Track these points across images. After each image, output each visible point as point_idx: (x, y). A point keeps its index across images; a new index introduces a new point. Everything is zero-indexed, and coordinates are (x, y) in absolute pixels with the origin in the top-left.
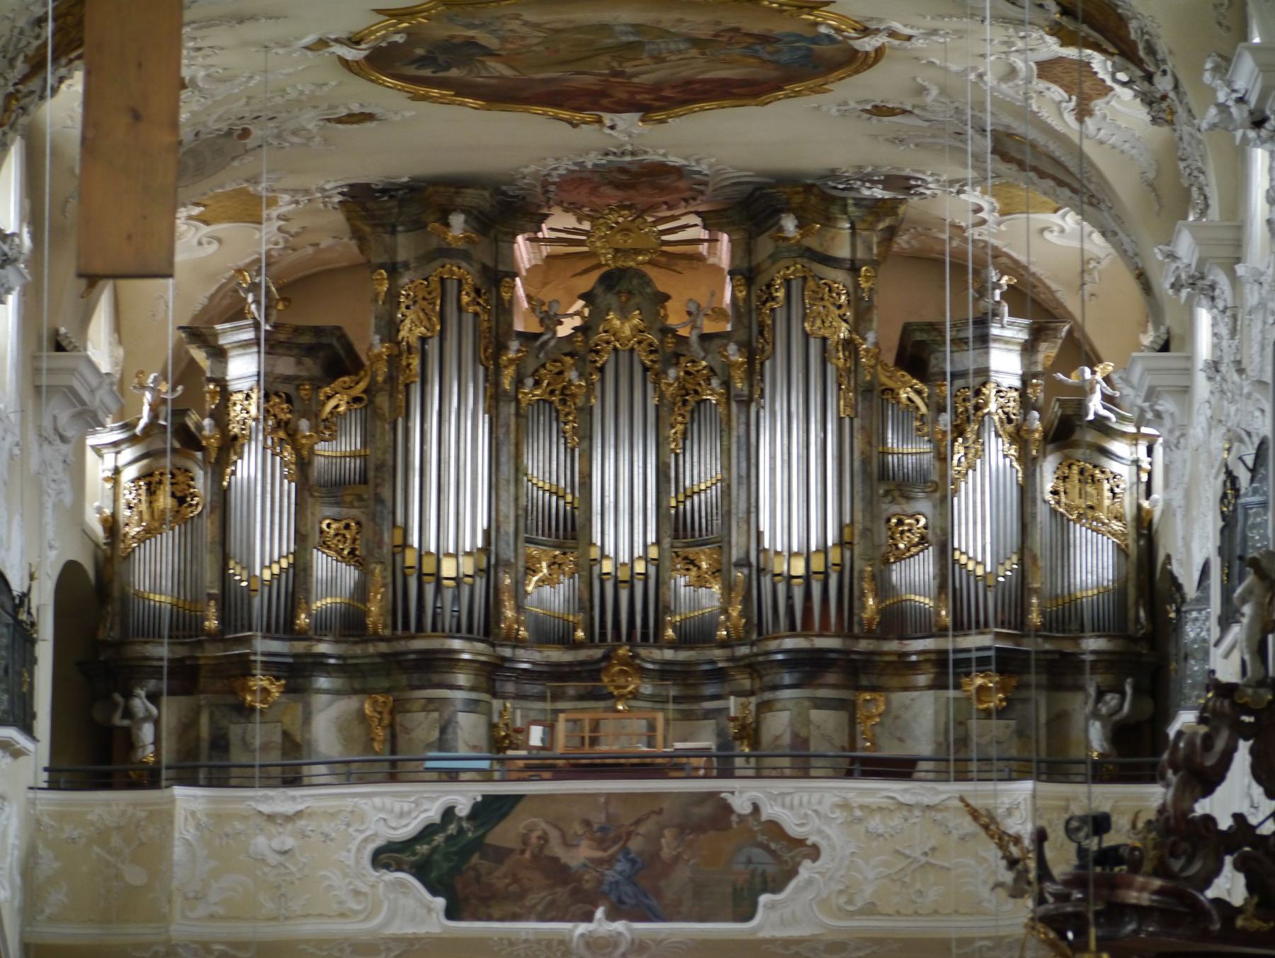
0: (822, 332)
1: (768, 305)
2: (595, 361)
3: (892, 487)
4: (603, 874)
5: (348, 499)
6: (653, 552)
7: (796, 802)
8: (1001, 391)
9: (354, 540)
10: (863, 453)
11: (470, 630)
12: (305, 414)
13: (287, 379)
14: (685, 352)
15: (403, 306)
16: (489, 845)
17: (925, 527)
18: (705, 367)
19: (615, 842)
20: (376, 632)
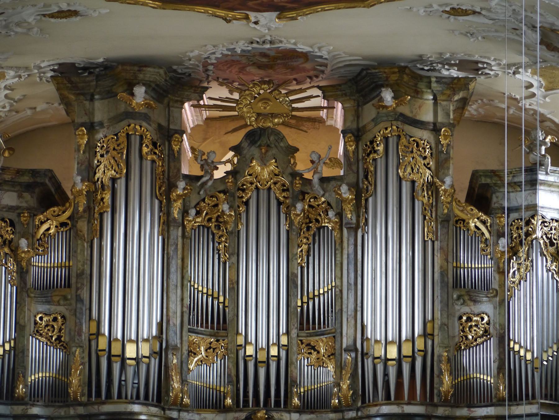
1: (371, 156)
2: (242, 197)
3: (463, 293)
5: (56, 299)
6: (284, 340)
8: (546, 222)
9: (60, 330)
10: (441, 267)
11: (146, 397)
12: (24, 235)
13: (11, 209)
14: (309, 191)
15: (99, 154)
17: (488, 323)
18: (324, 202)
20: (75, 399)
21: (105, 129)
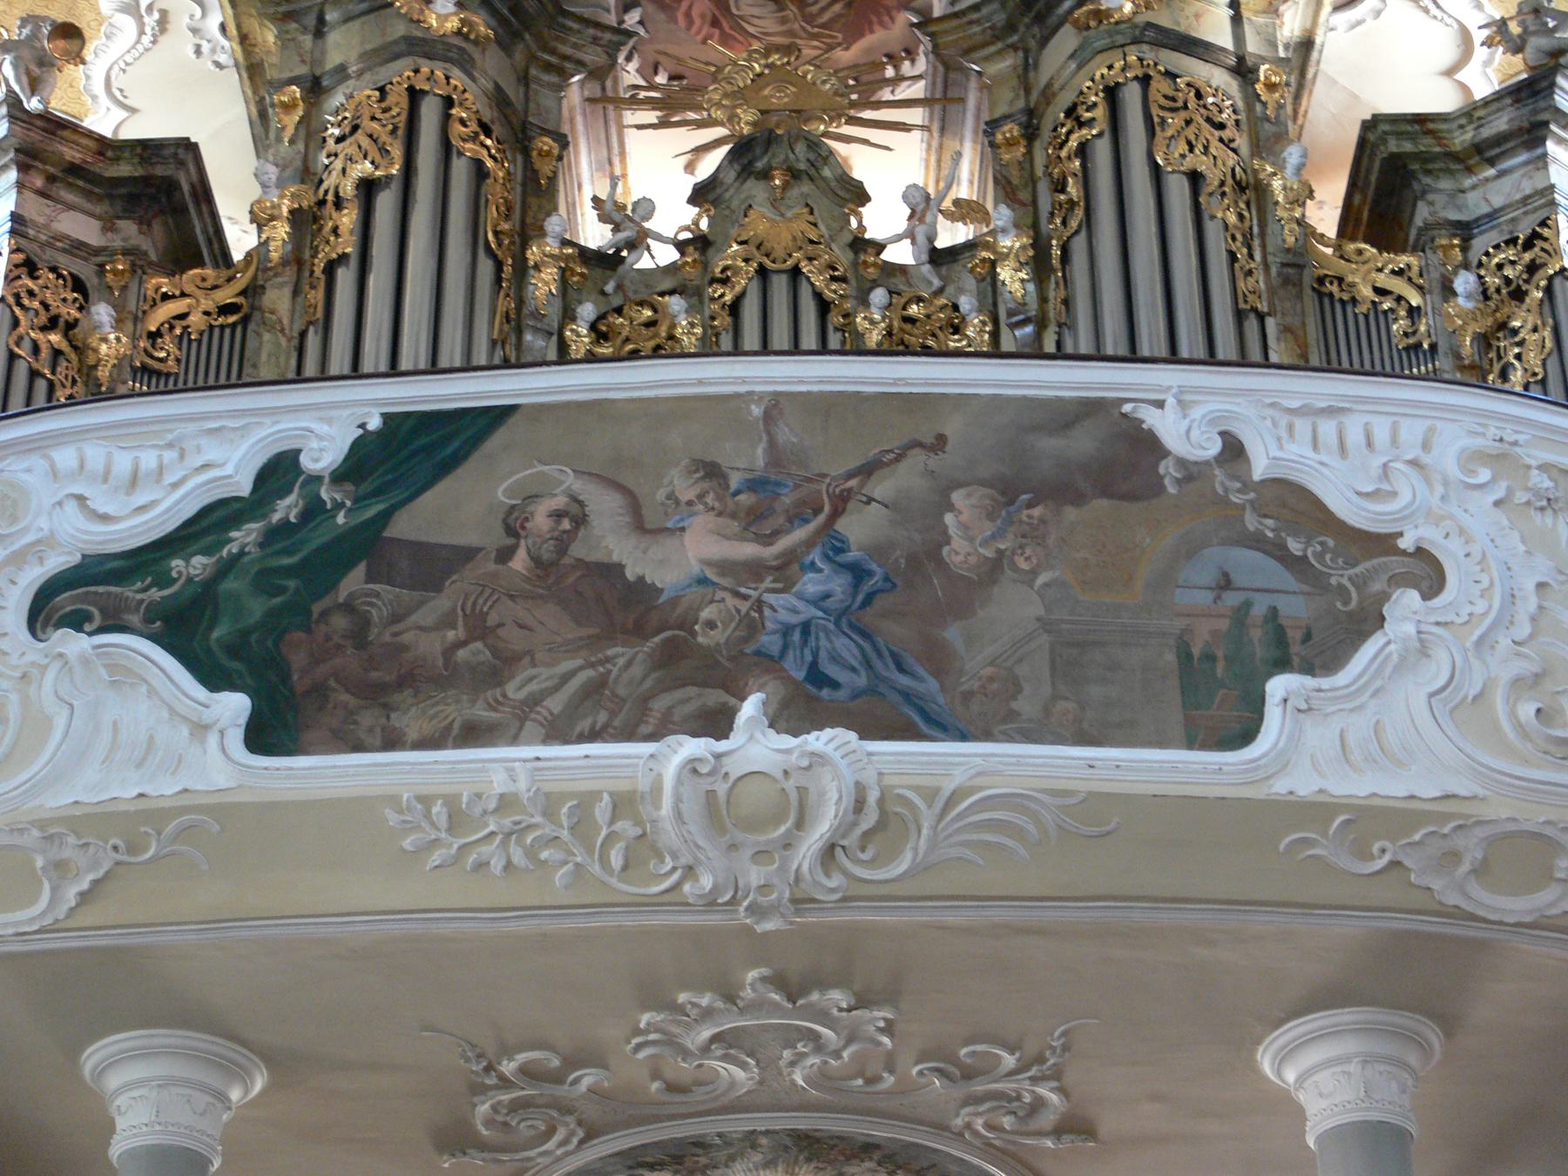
0: (1189, 162)
4: (759, 605)
7: (1355, 436)
13: (77, 248)
14: (902, 287)
15: (331, 142)
16: (392, 540)
19: (797, 517)
21: (351, 83)
